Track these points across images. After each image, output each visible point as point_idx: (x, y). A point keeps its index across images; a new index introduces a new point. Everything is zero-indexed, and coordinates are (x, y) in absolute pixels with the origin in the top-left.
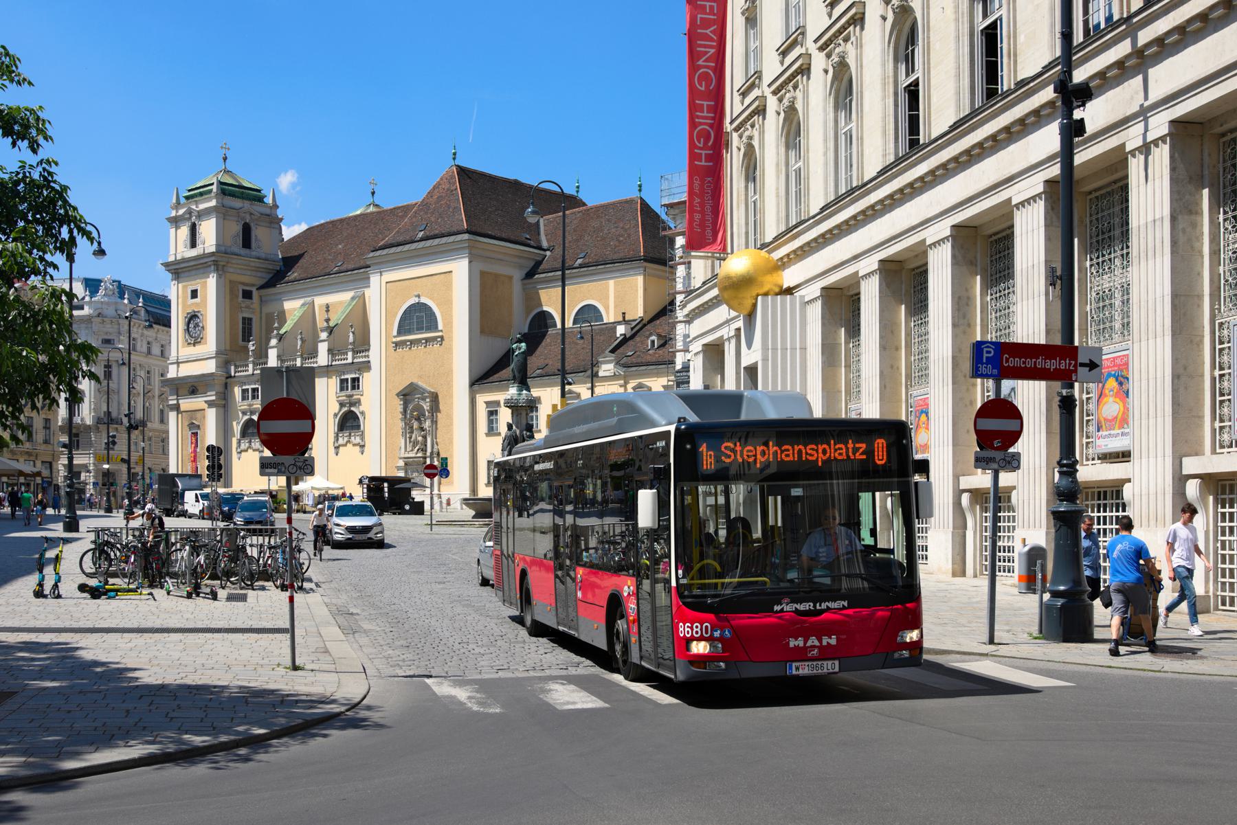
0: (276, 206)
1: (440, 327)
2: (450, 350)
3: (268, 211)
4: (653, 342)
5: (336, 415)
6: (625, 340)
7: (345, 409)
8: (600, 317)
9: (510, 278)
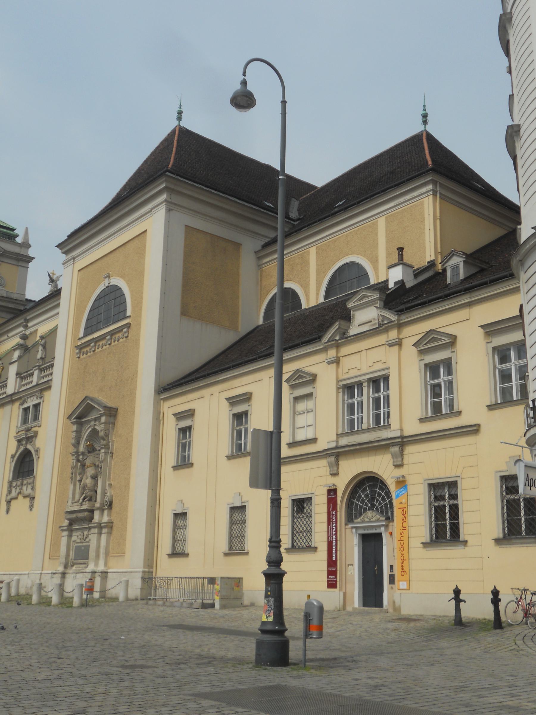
0: (26, 245)
1: (128, 313)
2: (137, 342)
3: (17, 250)
5: (13, 456)
7: (22, 448)
9: (237, 246)
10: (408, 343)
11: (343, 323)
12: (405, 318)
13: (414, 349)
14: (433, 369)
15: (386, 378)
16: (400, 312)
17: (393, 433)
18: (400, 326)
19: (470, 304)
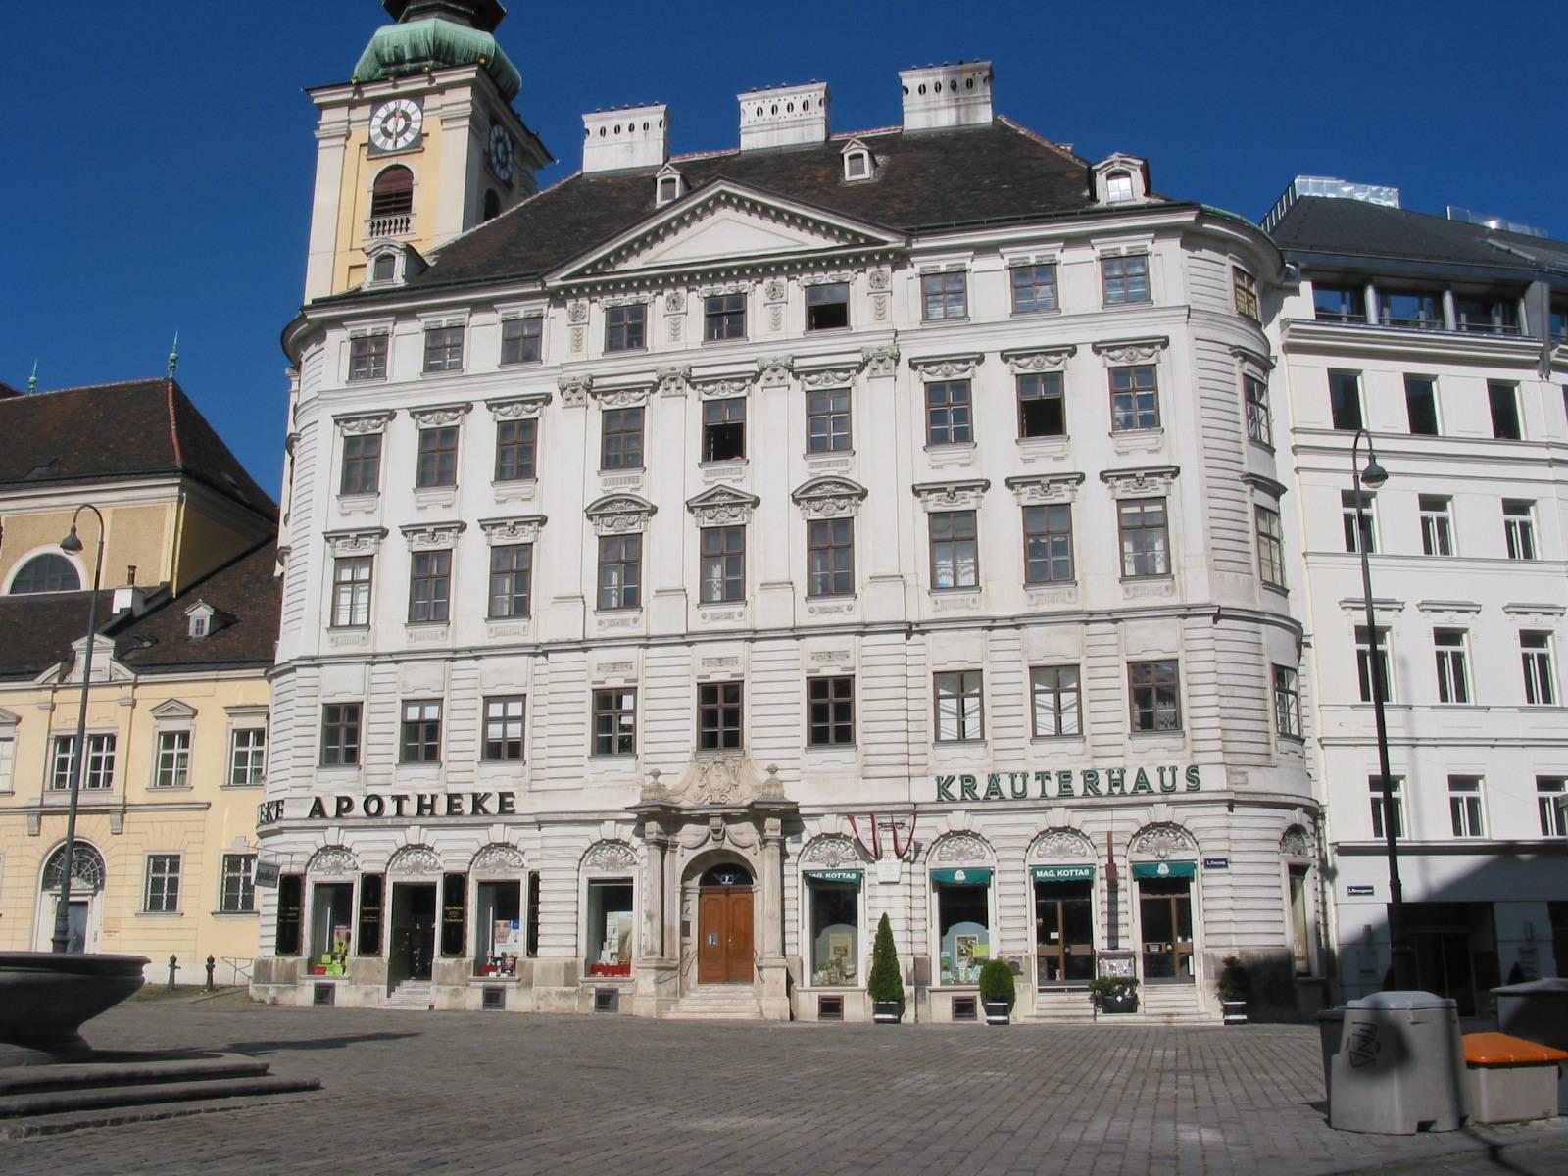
4: (200, 623)
6: (129, 619)
8: (72, 578)
10: (144, 706)
11: (66, 665)
12: (142, 678)
13: (151, 715)
14: (168, 739)
15: (112, 739)
16: (138, 674)
17: (114, 796)
18: (136, 685)
19: (217, 680)
